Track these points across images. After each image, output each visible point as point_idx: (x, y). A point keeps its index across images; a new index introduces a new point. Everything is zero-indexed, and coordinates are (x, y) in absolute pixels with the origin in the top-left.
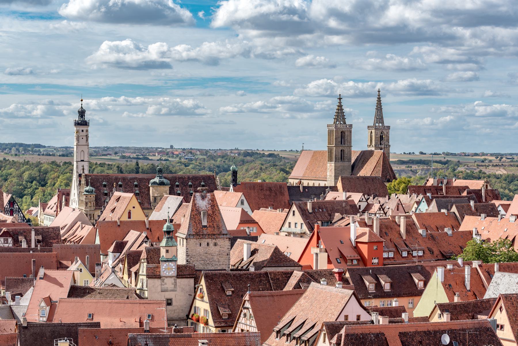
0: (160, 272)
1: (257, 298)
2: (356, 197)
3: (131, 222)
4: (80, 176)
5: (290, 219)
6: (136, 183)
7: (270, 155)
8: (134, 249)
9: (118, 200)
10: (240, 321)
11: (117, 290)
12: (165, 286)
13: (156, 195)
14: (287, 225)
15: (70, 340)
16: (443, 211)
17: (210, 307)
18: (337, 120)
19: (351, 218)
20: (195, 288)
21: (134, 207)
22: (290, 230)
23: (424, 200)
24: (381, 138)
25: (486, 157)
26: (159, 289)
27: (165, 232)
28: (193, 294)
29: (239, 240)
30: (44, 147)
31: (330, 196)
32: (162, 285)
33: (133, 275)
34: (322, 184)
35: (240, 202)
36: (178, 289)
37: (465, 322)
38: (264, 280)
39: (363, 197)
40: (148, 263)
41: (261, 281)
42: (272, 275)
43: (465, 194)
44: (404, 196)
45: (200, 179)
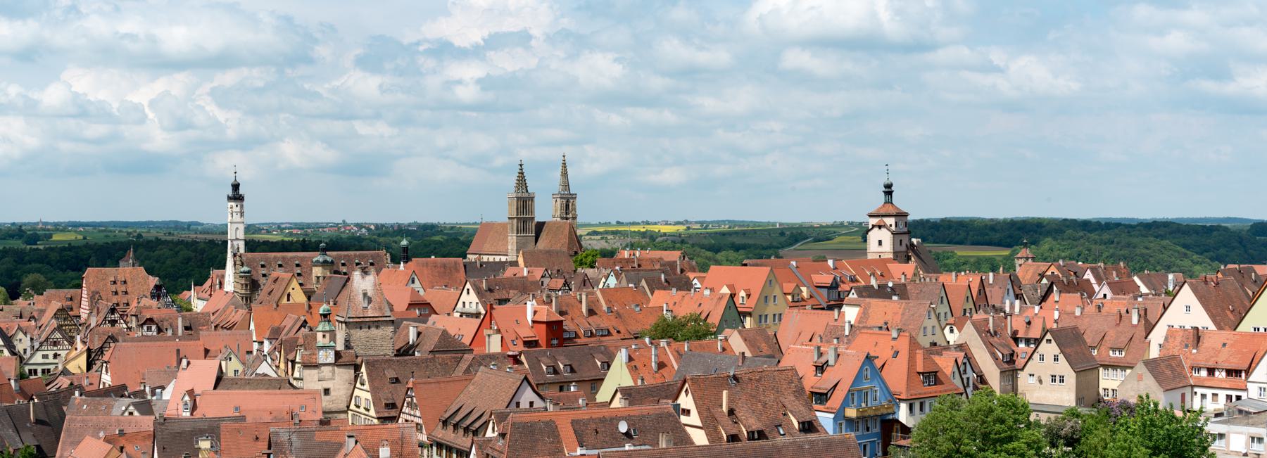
2: (538, 273)
4: (235, 255)
5: (464, 297)
7: (452, 228)
8: (291, 334)
9: (275, 281)
14: (460, 305)
24: (567, 206)
26: (316, 378)
31: (509, 272)
34: (503, 259)
36: (337, 377)
37: (648, 408)
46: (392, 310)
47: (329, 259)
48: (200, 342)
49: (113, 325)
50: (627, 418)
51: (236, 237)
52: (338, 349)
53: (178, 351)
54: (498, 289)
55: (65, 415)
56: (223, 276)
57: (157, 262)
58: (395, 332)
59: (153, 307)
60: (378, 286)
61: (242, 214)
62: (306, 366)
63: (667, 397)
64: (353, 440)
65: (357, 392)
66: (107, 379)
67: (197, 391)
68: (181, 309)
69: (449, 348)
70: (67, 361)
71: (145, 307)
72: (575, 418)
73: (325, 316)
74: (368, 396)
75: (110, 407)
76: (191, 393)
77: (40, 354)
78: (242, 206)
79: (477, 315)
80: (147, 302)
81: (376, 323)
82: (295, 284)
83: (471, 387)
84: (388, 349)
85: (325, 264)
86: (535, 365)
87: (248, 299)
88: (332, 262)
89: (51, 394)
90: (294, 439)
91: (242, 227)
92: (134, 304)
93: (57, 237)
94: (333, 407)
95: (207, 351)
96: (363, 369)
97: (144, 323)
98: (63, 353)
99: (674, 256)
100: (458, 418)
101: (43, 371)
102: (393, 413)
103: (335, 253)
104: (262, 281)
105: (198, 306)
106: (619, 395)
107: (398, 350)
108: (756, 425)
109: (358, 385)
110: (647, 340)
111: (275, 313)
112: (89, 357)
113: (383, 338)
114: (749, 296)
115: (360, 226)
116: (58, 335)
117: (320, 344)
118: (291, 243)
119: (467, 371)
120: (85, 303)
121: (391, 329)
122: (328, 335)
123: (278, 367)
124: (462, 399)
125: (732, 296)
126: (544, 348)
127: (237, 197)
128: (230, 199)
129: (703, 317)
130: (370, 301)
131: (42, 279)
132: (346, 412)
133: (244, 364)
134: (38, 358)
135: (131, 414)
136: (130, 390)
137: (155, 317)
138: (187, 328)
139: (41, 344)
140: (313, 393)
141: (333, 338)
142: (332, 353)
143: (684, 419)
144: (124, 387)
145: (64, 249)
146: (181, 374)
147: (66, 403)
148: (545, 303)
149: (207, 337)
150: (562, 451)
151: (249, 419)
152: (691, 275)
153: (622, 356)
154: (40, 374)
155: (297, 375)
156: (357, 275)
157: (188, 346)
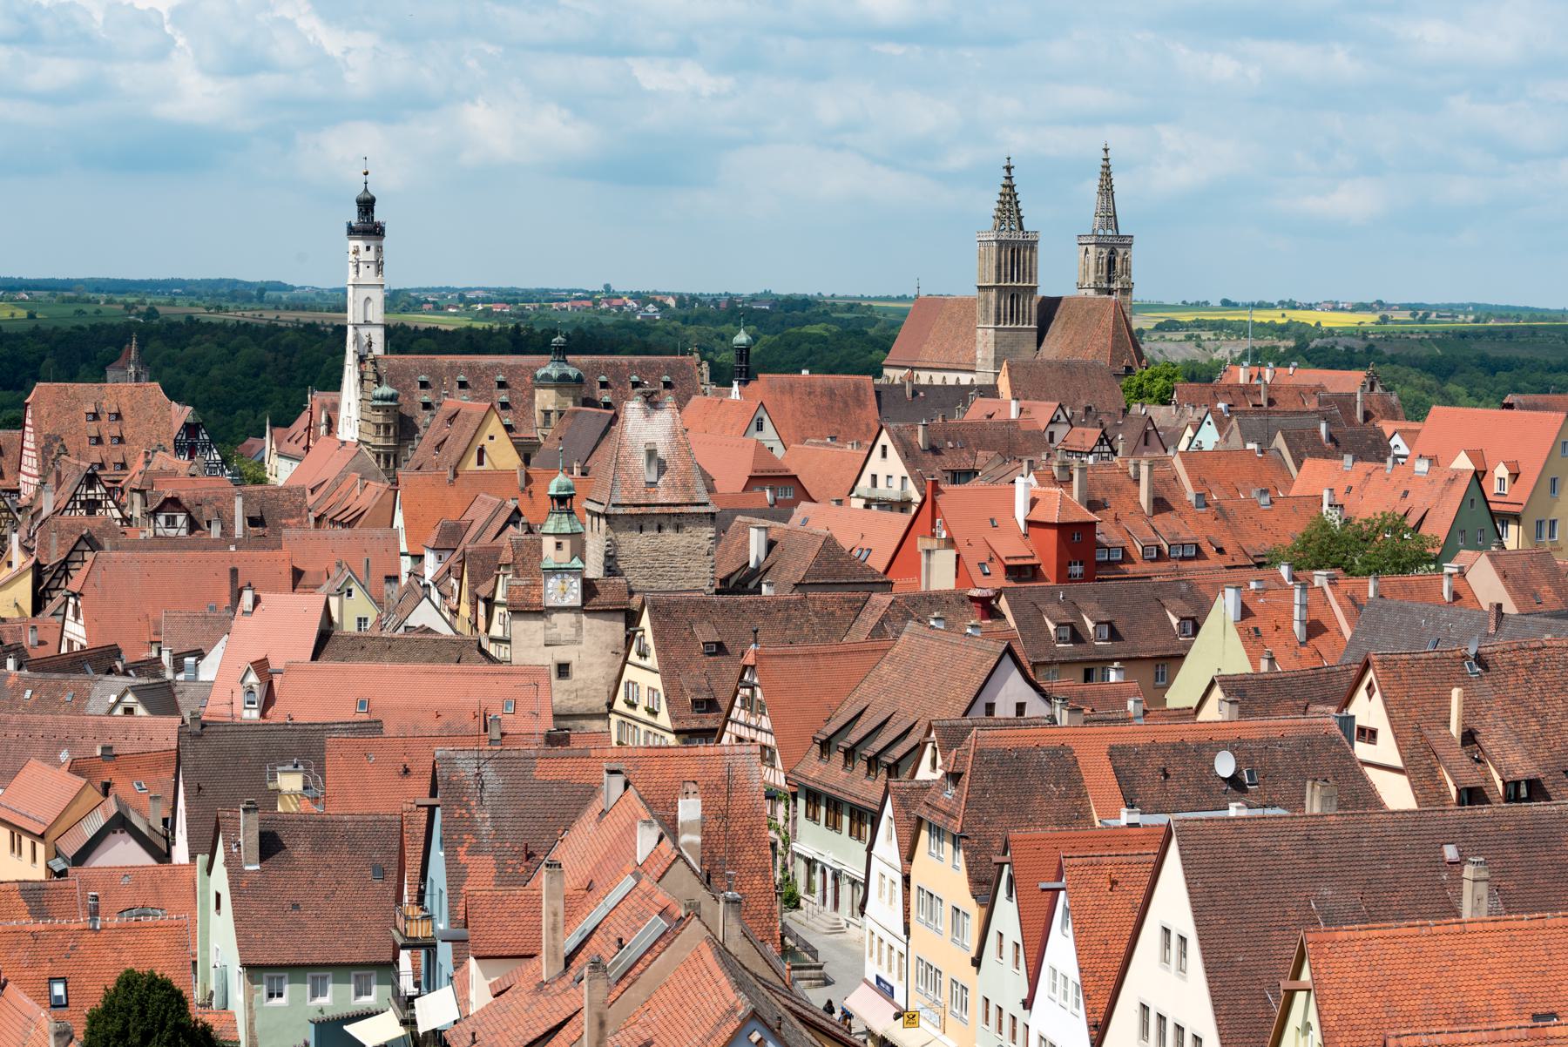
1: (775, 661)
2: (1043, 412)
4: (362, 360)
6: (501, 378)
7: (850, 308)
9: (452, 419)
13: (550, 407)
14: (865, 481)
15: (307, 766)
16: (1250, 446)
17: (663, 682)
18: (1002, 223)
19: (1025, 464)
20: (627, 637)
21: (491, 438)
22: (875, 494)
23: (1209, 418)
24: (1111, 263)
25: (1389, 314)
27: (552, 497)
29: (739, 518)
30: (293, 288)
31: (978, 410)
33: (482, 606)
34: (965, 379)
35: (754, 425)
36: (585, 637)
37: (1282, 724)
39: (1060, 412)
40: (517, 574)
41: (788, 619)
43: (1312, 405)
44: (1164, 408)
46: (711, 490)
47: (572, 372)
48: (282, 554)
49: (91, 512)
50: (1236, 747)
51: (365, 318)
52: (590, 574)
53: (234, 572)
54: (951, 447)
56: (335, 407)
57: (190, 371)
58: (717, 539)
59: (180, 474)
60: (681, 436)
61: (379, 266)
63: (1325, 700)
64: (618, 781)
65: (630, 673)
66: (76, 632)
67: (275, 664)
68: (241, 479)
69: (840, 578)
71: (163, 473)
72: (1118, 741)
73: (561, 500)
74: (656, 681)
75: (82, 696)
76: (261, 666)
78: (379, 250)
79: (903, 505)
80: (166, 460)
81: (675, 519)
82: (495, 426)
83: (885, 668)
84: (700, 578)
85: (562, 383)
86: (1030, 620)
87: (391, 459)
88: (579, 380)
90: (489, 773)
91: (378, 297)
92: (137, 466)
94: (578, 704)
95: (297, 574)
96: (645, 622)
99: (1350, 381)
100: (854, 737)
102: (710, 721)
103: (584, 359)
104: (423, 418)
105: (280, 472)
106: (1217, 693)
107: (724, 581)
108: (1524, 769)
109: (633, 657)
110: (1284, 571)
112: (37, 581)
113: (690, 553)
114: (1515, 476)
115: (642, 298)
118: (489, 333)
119: (878, 631)
120: (30, 463)
121: (708, 532)
122: (566, 543)
123: (455, 612)
124: (865, 694)
125: (1479, 476)
126: (1052, 583)
127: (368, 226)
128: (352, 231)
129: (1411, 521)
130: (662, 468)
132: (604, 717)
133: (379, 603)
135: (129, 711)
136: (128, 657)
137: (184, 496)
138: (253, 522)
140: (533, 674)
141: (579, 551)
142: (577, 584)
143: (1362, 750)
144: (115, 652)
146: (239, 623)
148: (1055, 482)
149: (300, 543)
150: (1085, 816)
151: (390, 729)
152: (1387, 427)
153: (1226, 605)
155: (497, 630)
156: (633, 409)
157: (254, 562)
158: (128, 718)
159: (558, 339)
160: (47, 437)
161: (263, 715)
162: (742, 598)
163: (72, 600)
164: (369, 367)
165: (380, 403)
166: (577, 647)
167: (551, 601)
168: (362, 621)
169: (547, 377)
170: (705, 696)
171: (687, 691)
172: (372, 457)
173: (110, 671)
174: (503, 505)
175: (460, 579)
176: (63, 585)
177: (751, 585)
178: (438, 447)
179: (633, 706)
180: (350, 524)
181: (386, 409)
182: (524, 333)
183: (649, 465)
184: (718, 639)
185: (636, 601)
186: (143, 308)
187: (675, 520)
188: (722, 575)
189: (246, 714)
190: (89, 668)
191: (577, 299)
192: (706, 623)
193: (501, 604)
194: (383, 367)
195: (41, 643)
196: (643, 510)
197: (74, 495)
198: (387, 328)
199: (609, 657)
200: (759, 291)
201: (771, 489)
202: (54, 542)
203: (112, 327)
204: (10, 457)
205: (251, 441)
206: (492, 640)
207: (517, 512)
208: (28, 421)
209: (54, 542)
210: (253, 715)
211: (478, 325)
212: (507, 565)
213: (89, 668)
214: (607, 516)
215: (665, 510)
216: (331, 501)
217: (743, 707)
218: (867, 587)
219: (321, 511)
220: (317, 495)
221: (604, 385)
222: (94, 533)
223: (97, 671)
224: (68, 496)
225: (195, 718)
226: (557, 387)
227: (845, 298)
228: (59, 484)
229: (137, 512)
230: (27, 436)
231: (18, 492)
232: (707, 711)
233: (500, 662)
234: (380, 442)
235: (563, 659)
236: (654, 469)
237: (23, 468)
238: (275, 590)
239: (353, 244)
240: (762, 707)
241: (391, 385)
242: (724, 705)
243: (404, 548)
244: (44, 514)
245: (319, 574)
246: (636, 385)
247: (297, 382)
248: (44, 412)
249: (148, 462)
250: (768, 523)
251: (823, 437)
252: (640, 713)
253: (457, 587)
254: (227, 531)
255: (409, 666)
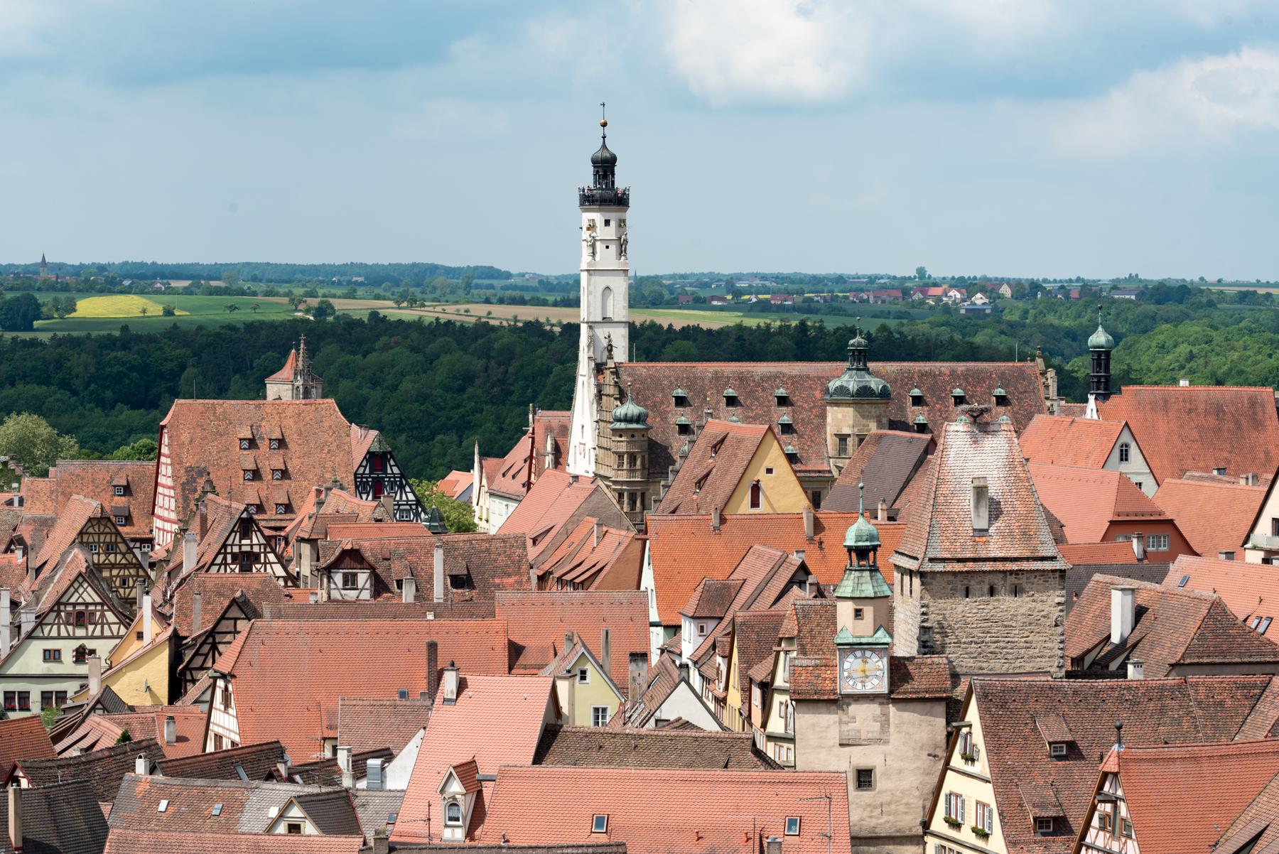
0: (834, 681)
1: (1145, 766)
3: (758, 517)
4: (599, 369)
6: (781, 392)
9: (717, 446)
10: (1088, 840)
11: (696, 739)
12: (851, 726)
13: (846, 431)
20: (949, 735)
21: (769, 471)
26: (833, 736)
27: (850, 549)
28: (942, 754)
29: (1097, 577)
30: (508, 275)
32: (841, 722)
33: (756, 693)
35: (1116, 454)
36: (894, 736)
38: (1172, 710)
40: (803, 651)
41: (1162, 711)
42: (1202, 689)
45: (990, 378)
46: (1059, 539)
47: (875, 384)
49: (246, 569)
51: (603, 317)
52: (900, 651)
53: (432, 647)
55: (105, 828)
56: (565, 430)
57: (375, 384)
58: (1067, 606)
59: (360, 518)
60: (1019, 467)
61: (622, 251)
62: (806, 700)
65: (953, 782)
66: (227, 726)
67: (485, 769)
68: (439, 524)
70: (113, 670)
71: (339, 517)
73: (862, 553)
74: (986, 793)
75: (234, 808)
77: (35, 649)
78: (622, 223)
80: (345, 501)
82: (774, 456)
87: (637, 499)
88: (885, 394)
89: (67, 764)
91: (620, 287)
92: (306, 508)
93: (91, 307)
94: (883, 824)
95: (515, 651)
96: (973, 715)
97: (336, 565)
98: (103, 648)
101: (46, 696)
103: (892, 367)
104: (678, 445)
105: (493, 516)
107: (1077, 661)
109: (957, 761)
111: (716, 544)
112: (175, 659)
113: (1032, 623)
115: (969, 286)
116: (89, 595)
117: (845, 637)
118: (765, 333)
120: (167, 503)
121: (1057, 596)
122: (868, 611)
127: (606, 193)
128: (588, 200)
130: (995, 511)
131: (44, 430)
132: (918, 840)
133: (621, 689)
134: (31, 660)
135: (294, 828)
136: (293, 758)
138: (459, 581)
139: (41, 620)
140: (824, 782)
141: (886, 622)
142: (883, 664)
144: (275, 751)
145: (108, 343)
146: (439, 714)
147: (110, 793)
149: (517, 610)
154: (35, 706)
155: (776, 725)
156: (956, 433)
158: (294, 838)
159: (857, 340)
160: (189, 470)
161: (470, 834)
162: (1101, 683)
163: (220, 683)
164: (609, 378)
165: (623, 426)
166: (883, 748)
167: (848, 688)
168: (599, 712)
169: (842, 390)
170: (1051, 813)
171: (1028, 807)
172: (612, 497)
173: (270, 776)
174: (784, 560)
175: (729, 658)
176: (209, 664)
177: (1113, 666)
178: (700, 483)
179: (956, 825)
180: (583, 585)
181: (632, 433)
182: (812, 333)
183: (977, 506)
184: (1069, 738)
185: (960, 692)
186: (314, 302)
187: (1011, 579)
188: (1075, 653)
189: (447, 834)
190: (241, 771)
191: (884, 287)
192: (1053, 717)
193: (782, 691)
194: (626, 378)
195: (180, 739)
196: (970, 566)
197: (224, 546)
198: (631, 326)
199: (925, 761)
200: (1123, 275)
201: (1140, 537)
202: (198, 606)
203: (273, 326)
204: (141, 496)
205: (454, 475)
206: (771, 738)
207: (803, 568)
208: (165, 450)
209: (198, 606)
210: (456, 835)
211: (752, 322)
212: (790, 639)
213: (241, 771)
214: (922, 575)
215: (1000, 566)
216: (559, 554)
217: (1102, 828)
218: (1268, 669)
219: (546, 567)
220: (542, 546)
221: (917, 401)
222: (250, 596)
223: (252, 776)
224: (217, 547)
225: (381, 838)
226: (855, 404)
227: (1236, 284)
228: (204, 531)
229: (306, 570)
230: (163, 469)
231: (150, 541)
232: (1055, 833)
233: (782, 768)
234: (623, 476)
235: (864, 763)
236: (984, 513)
237: (158, 511)
238: (487, 671)
239: (587, 217)
240: (1128, 827)
241: (637, 401)
242: (1077, 826)
243: (654, 616)
244: (184, 572)
245: (543, 650)
246: (960, 400)
247: (514, 398)
248: (185, 437)
249: (320, 504)
250: (1135, 584)
251: (1208, 470)
252: (966, 835)
253: (724, 668)
254: (422, 594)
255: (661, 772)
